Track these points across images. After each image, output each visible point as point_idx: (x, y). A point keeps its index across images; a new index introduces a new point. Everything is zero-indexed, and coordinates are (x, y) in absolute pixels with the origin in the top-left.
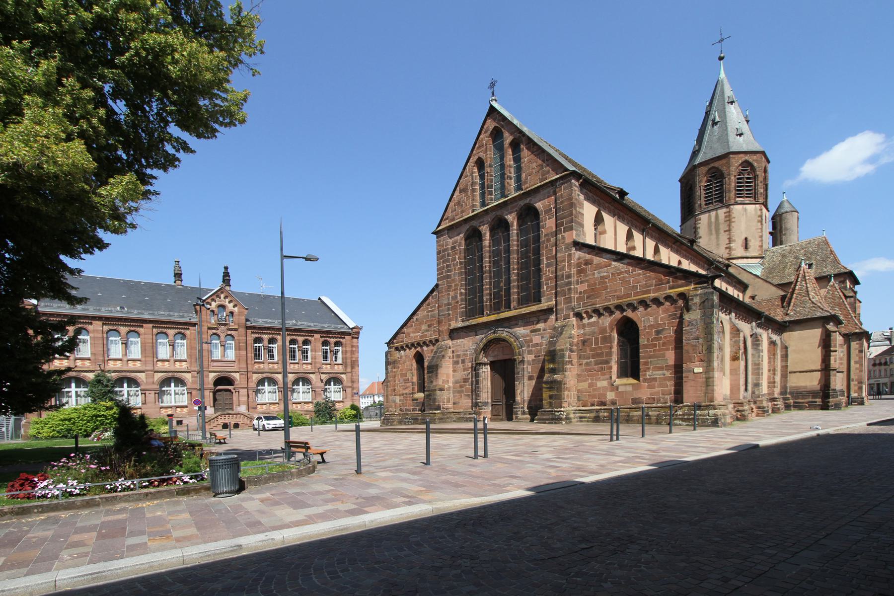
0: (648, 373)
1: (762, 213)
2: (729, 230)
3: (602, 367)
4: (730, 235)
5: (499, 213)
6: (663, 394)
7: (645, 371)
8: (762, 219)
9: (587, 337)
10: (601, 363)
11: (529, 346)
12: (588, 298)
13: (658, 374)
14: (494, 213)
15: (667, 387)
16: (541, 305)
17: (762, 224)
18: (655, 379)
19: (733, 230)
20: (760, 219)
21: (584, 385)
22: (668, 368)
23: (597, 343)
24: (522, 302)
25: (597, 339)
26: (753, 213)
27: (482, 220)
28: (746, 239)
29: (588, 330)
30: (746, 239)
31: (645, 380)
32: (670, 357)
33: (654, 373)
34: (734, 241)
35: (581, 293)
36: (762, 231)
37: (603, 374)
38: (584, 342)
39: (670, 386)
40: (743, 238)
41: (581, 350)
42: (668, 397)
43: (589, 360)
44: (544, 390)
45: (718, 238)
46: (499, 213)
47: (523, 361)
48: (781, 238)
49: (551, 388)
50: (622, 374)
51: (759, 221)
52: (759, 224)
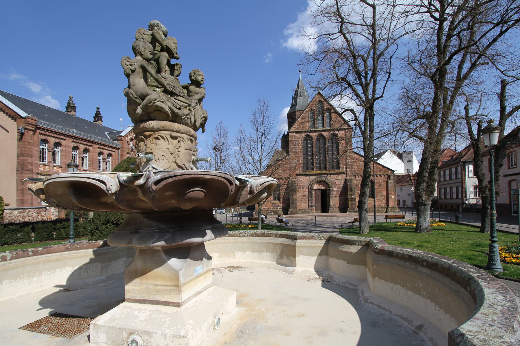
0: (378, 197)
11: (334, 185)
13: (380, 197)
18: (379, 199)
22: (383, 196)
32: (385, 193)
35: (355, 169)
47: (333, 190)
49: (352, 201)
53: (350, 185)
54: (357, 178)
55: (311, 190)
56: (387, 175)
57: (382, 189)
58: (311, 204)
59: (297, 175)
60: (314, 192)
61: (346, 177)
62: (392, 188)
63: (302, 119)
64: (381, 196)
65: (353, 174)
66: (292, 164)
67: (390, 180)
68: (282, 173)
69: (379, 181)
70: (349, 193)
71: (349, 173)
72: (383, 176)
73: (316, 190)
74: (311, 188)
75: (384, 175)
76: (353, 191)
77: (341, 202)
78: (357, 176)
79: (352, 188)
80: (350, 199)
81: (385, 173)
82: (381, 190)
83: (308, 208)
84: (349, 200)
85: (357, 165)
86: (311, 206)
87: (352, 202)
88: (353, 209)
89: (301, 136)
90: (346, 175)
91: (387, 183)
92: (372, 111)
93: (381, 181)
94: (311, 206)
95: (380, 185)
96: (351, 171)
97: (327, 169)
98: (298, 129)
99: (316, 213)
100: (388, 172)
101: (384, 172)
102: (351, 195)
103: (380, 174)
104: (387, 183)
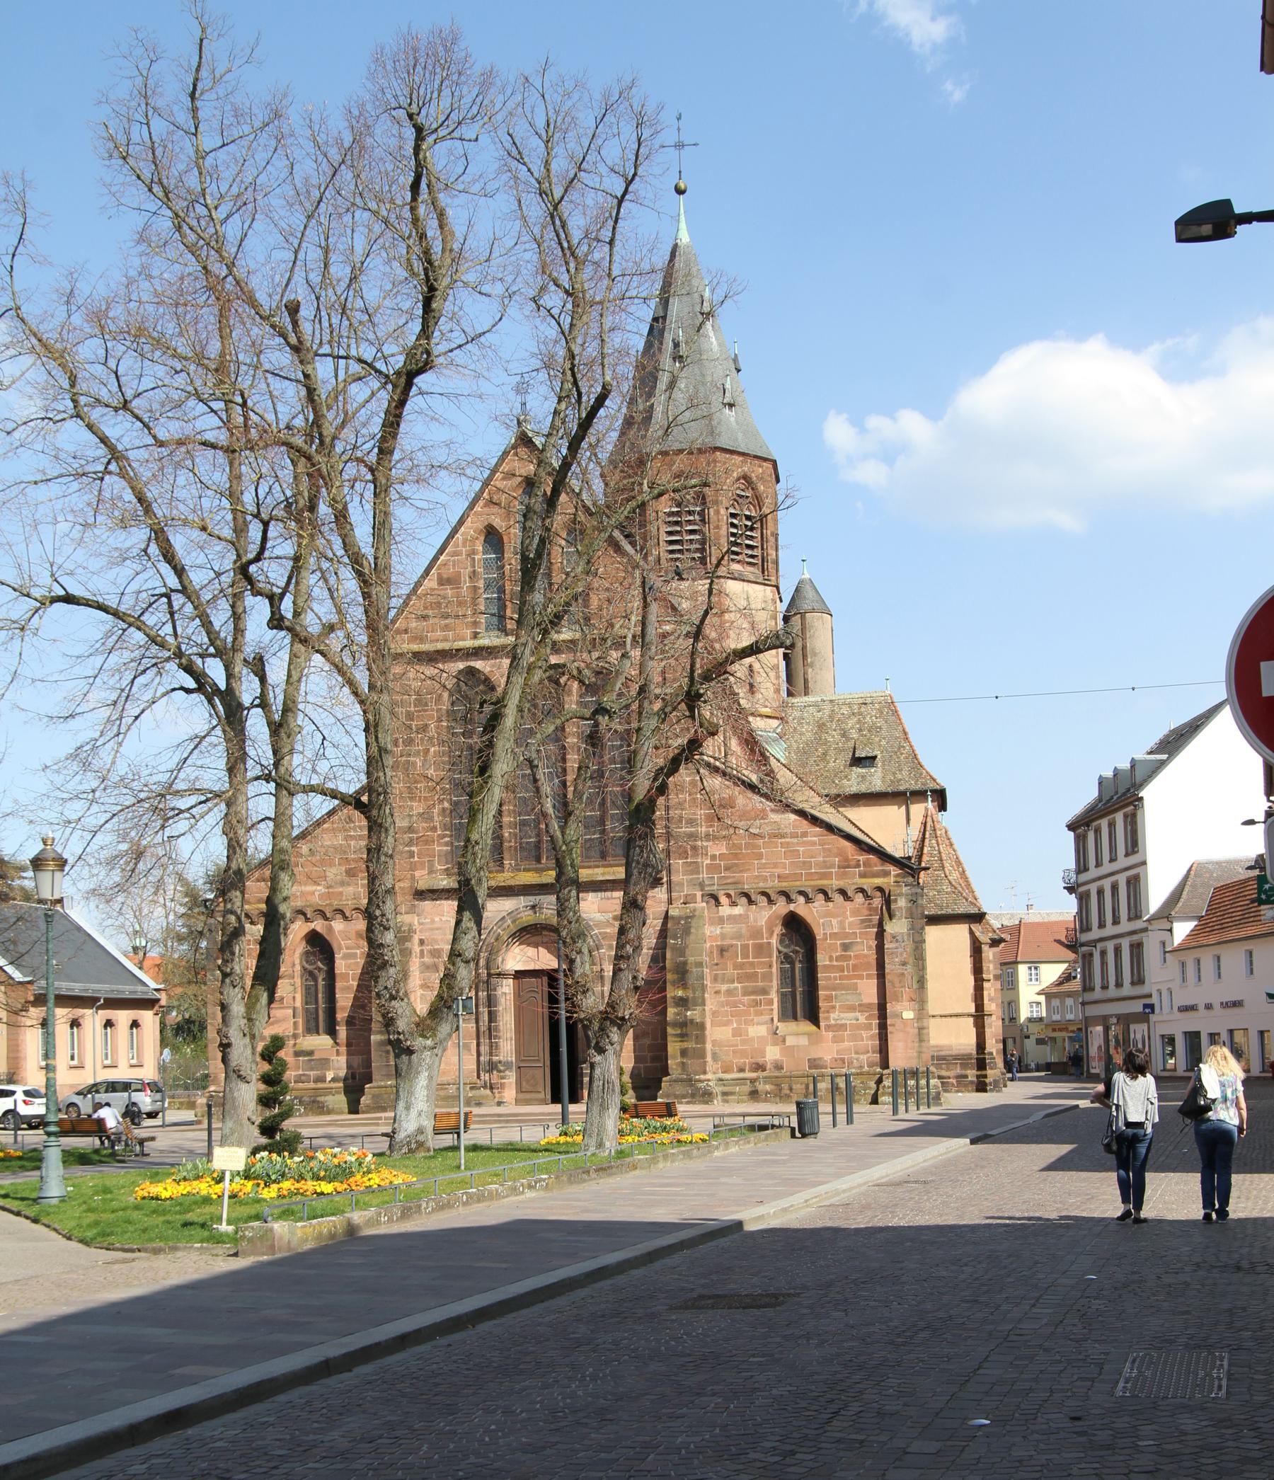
0: (832, 1015)
6: (857, 1053)
10: (753, 993)
13: (848, 1018)
18: (842, 1025)
22: (863, 1007)
23: (745, 956)
25: (745, 947)
29: (728, 928)
31: (829, 1028)
33: (842, 1015)
37: (761, 1013)
38: (722, 950)
39: (869, 1039)
42: (864, 1057)
44: (669, 1038)
48: (805, 673)
49: (683, 1036)
50: (789, 1013)
53: (681, 951)
54: (726, 910)
55: (489, 975)
56: (880, 889)
57: (855, 967)
58: (491, 1054)
59: (421, 895)
60: (506, 989)
61: (670, 902)
62: (904, 964)
63: (442, 581)
64: (851, 1008)
65: (702, 886)
67: (891, 917)
68: (342, 884)
69: (841, 923)
70: (673, 992)
72: (859, 898)
73: (519, 975)
74: (488, 968)
75: (862, 891)
76: (691, 980)
77: (647, 1041)
78: (723, 900)
79: (685, 963)
80: (676, 1024)
81: (868, 883)
82: (848, 977)
83: (479, 1077)
84: (669, 1030)
86: (492, 1067)
87: (685, 1045)
88: (690, 1080)
90: (670, 891)
91: (880, 935)
93: (850, 924)
94: (492, 1067)
95: (846, 947)
96: (694, 868)
98: (421, 639)
99: (518, 1102)
100: (887, 874)
101: (863, 875)
102: (683, 1003)
104: (880, 935)
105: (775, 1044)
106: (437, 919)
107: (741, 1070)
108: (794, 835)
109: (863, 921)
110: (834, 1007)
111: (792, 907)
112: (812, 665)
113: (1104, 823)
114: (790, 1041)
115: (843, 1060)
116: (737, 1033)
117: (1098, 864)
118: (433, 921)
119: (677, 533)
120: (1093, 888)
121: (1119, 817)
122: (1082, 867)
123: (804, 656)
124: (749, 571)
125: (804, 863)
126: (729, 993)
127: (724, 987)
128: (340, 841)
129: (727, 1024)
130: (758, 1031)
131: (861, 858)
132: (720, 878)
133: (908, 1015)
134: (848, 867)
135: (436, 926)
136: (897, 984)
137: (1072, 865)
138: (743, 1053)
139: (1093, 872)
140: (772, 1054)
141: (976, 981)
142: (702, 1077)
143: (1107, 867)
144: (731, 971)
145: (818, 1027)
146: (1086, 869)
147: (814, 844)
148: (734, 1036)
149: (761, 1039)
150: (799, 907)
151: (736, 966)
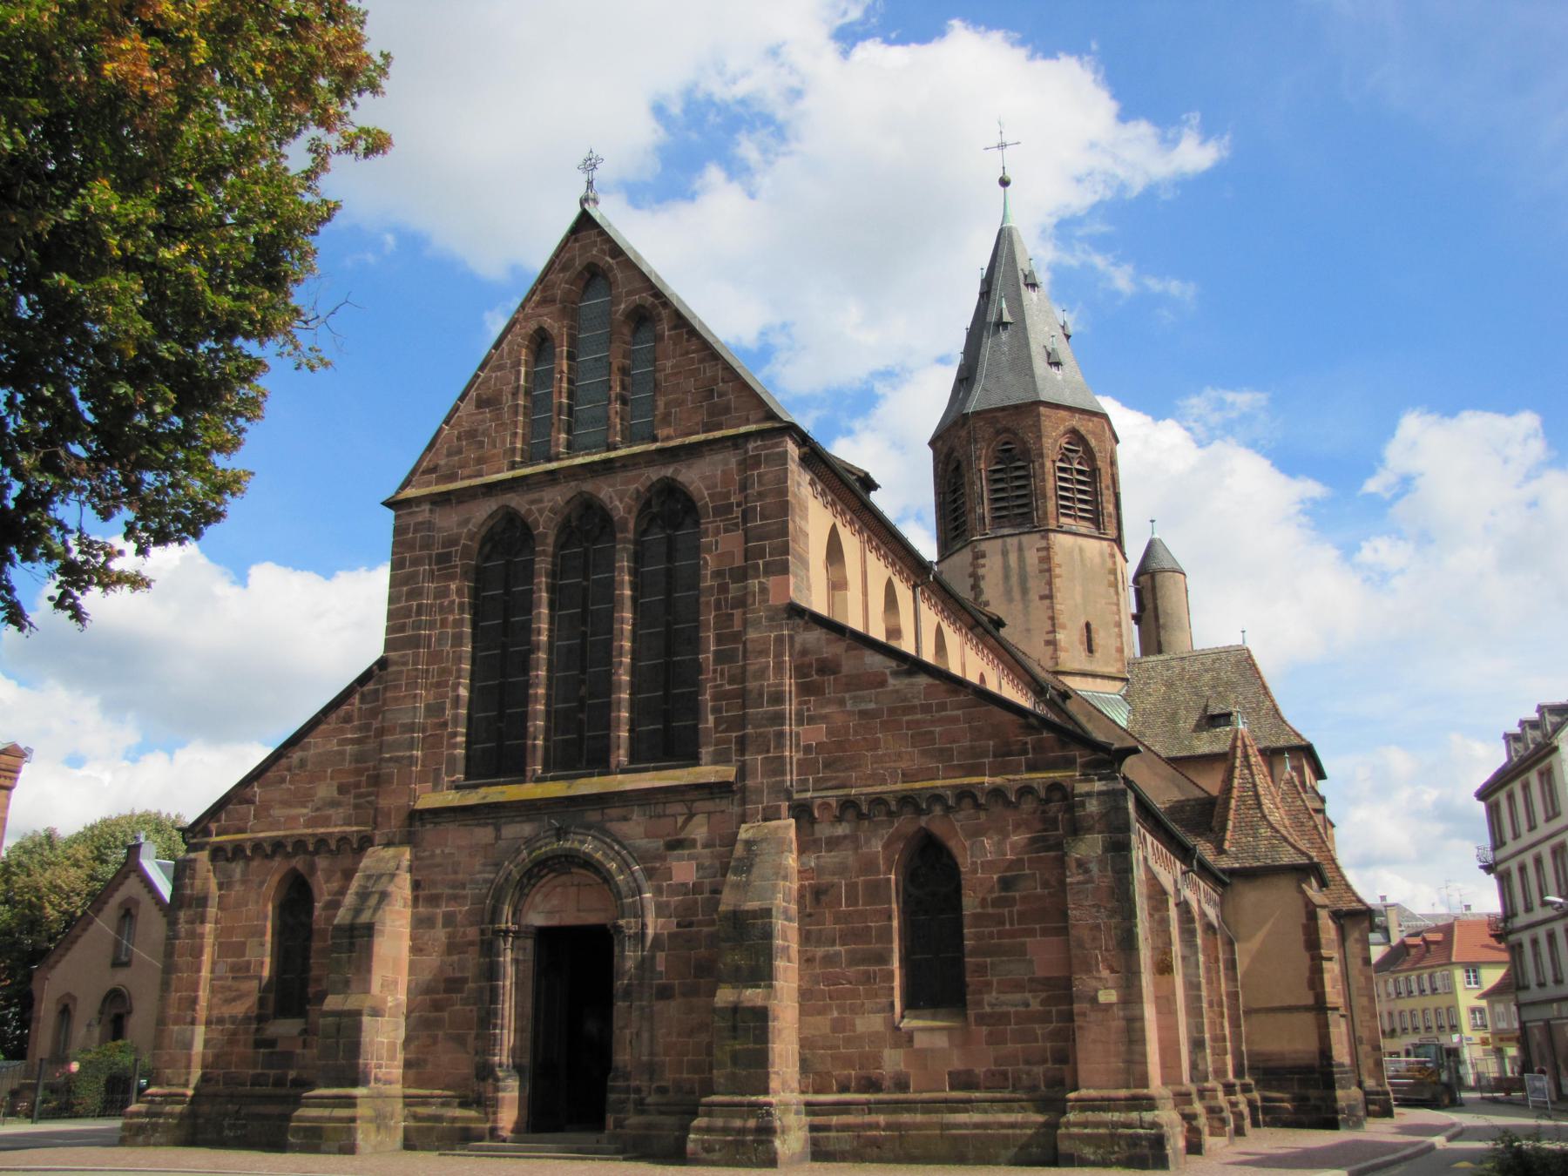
0: (986, 997)
1: (1114, 563)
2: (1050, 597)
3: (867, 973)
4: (1052, 608)
5: (588, 487)
6: (1027, 1062)
7: (980, 992)
8: (1116, 579)
9: (827, 879)
10: (863, 961)
12: (827, 765)
13: (1011, 1002)
14: (573, 484)
15: (1036, 1040)
16: (697, 769)
17: (1117, 593)
18: (1003, 1018)
19: (1059, 596)
20: (1112, 578)
21: (822, 1024)
23: (851, 900)
24: (642, 757)
25: (852, 888)
26: (1097, 560)
27: (536, 496)
28: (1088, 625)
29: (829, 858)
30: (1088, 625)
31: (982, 1019)
33: (1003, 997)
34: (1064, 627)
36: (1119, 610)
40: (1082, 623)
41: (810, 915)
42: (1038, 1070)
43: (832, 950)
45: (1026, 613)
46: (588, 487)
51: (1110, 585)
52: (1112, 590)
56: (1054, 787)
57: (1021, 914)
64: (1018, 986)
66: (392, 730)
68: (334, 804)
71: (759, 791)
82: (1012, 934)
85: (824, 718)
89: (467, 521)
92: (988, 298)
97: (622, 756)
100: (1068, 763)
101: (1032, 768)
103: (998, 780)
105: (896, 1046)
106: (438, 851)
107: (844, 1089)
108: (926, 709)
109: (1033, 841)
110: (988, 984)
111: (923, 821)
112: (1164, 627)
113: (1517, 786)
114: (920, 1041)
115: (1004, 1074)
116: (838, 1026)
117: (1516, 836)
118: (433, 856)
119: (1002, 490)
120: (1513, 865)
121: (1533, 777)
122: (1498, 842)
123: (1157, 617)
124: (1083, 527)
125: (941, 751)
126: (829, 960)
127: (820, 952)
128: (333, 746)
129: (822, 1011)
130: (870, 1023)
131: (1029, 739)
132: (816, 781)
133: (1108, 996)
134: (1010, 754)
135: (438, 860)
136: (1088, 946)
137: (1486, 841)
138: (848, 1062)
139: (1511, 846)
140: (892, 1061)
141: (1313, 958)
142: (762, 1099)
143: (1527, 838)
144: (829, 926)
145: (965, 1017)
146: (1503, 844)
147: (955, 720)
148: (834, 1030)
149: (875, 1038)
150: (935, 822)
151: (837, 920)
